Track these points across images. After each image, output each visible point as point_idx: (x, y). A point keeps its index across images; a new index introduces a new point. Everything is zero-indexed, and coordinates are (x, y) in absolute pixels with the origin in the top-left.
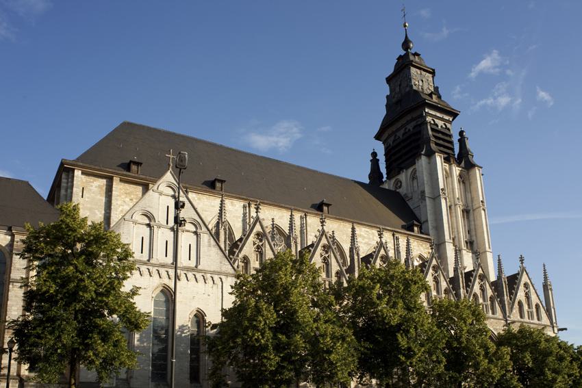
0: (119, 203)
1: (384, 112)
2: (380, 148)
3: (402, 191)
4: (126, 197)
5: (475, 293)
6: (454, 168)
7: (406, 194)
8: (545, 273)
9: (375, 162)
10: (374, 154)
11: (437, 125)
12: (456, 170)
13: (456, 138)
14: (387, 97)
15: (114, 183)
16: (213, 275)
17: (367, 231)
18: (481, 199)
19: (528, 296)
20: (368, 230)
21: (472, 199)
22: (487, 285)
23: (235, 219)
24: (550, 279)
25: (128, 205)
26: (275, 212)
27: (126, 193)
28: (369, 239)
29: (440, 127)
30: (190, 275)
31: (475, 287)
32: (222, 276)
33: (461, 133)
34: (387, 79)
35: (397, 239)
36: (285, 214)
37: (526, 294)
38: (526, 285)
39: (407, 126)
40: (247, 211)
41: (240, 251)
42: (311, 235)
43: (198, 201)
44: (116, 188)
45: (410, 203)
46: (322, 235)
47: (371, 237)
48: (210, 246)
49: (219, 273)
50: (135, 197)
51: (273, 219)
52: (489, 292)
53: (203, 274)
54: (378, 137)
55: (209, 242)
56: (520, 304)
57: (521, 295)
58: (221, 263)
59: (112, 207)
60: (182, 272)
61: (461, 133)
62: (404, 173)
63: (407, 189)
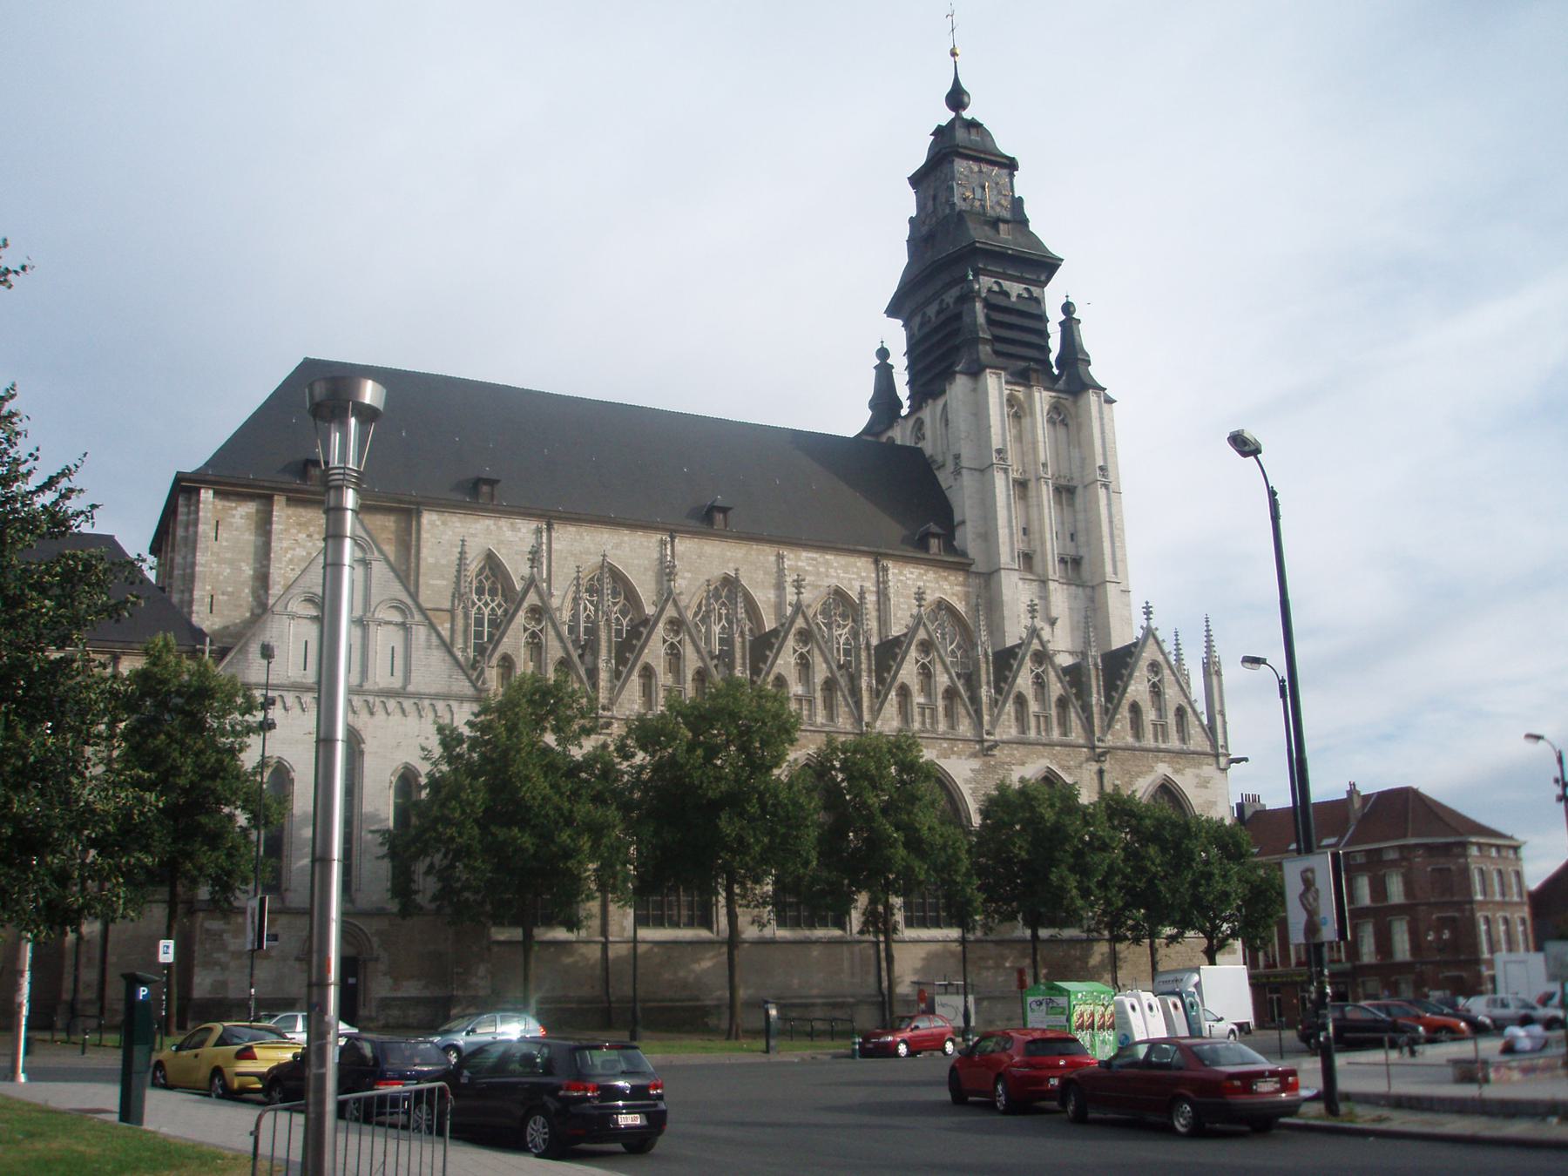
0: (285, 544)
1: (902, 259)
2: (896, 336)
3: (928, 447)
4: (299, 532)
6: (1037, 395)
7: (931, 456)
8: (1208, 636)
9: (884, 372)
10: (883, 353)
11: (1006, 294)
12: (1042, 399)
13: (1054, 317)
14: (912, 220)
15: (276, 508)
16: (434, 702)
17: (813, 559)
18: (1100, 462)
19: (1156, 691)
20: (815, 555)
21: (1083, 460)
22: (1052, 674)
23: (519, 557)
25: (304, 547)
26: (606, 536)
27: (299, 524)
28: (818, 574)
29: (1014, 299)
30: (392, 704)
31: (1019, 681)
32: (452, 703)
33: (1068, 308)
35: (885, 569)
36: (626, 538)
37: (1154, 685)
38: (1154, 667)
39: (944, 297)
40: (544, 539)
41: (494, 650)
42: (684, 578)
43: (441, 528)
44: (279, 516)
46: (667, 600)
47: (822, 570)
48: (429, 647)
49: (446, 697)
51: (578, 567)
52: (1056, 689)
53: (416, 701)
54: (893, 310)
55: (428, 640)
56: (1135, 708)
57: (1138, 689)
58: (450, 677)
59: (272, 555)
60: (378, 700)
61: (1068, 308)
62: (928, 408)
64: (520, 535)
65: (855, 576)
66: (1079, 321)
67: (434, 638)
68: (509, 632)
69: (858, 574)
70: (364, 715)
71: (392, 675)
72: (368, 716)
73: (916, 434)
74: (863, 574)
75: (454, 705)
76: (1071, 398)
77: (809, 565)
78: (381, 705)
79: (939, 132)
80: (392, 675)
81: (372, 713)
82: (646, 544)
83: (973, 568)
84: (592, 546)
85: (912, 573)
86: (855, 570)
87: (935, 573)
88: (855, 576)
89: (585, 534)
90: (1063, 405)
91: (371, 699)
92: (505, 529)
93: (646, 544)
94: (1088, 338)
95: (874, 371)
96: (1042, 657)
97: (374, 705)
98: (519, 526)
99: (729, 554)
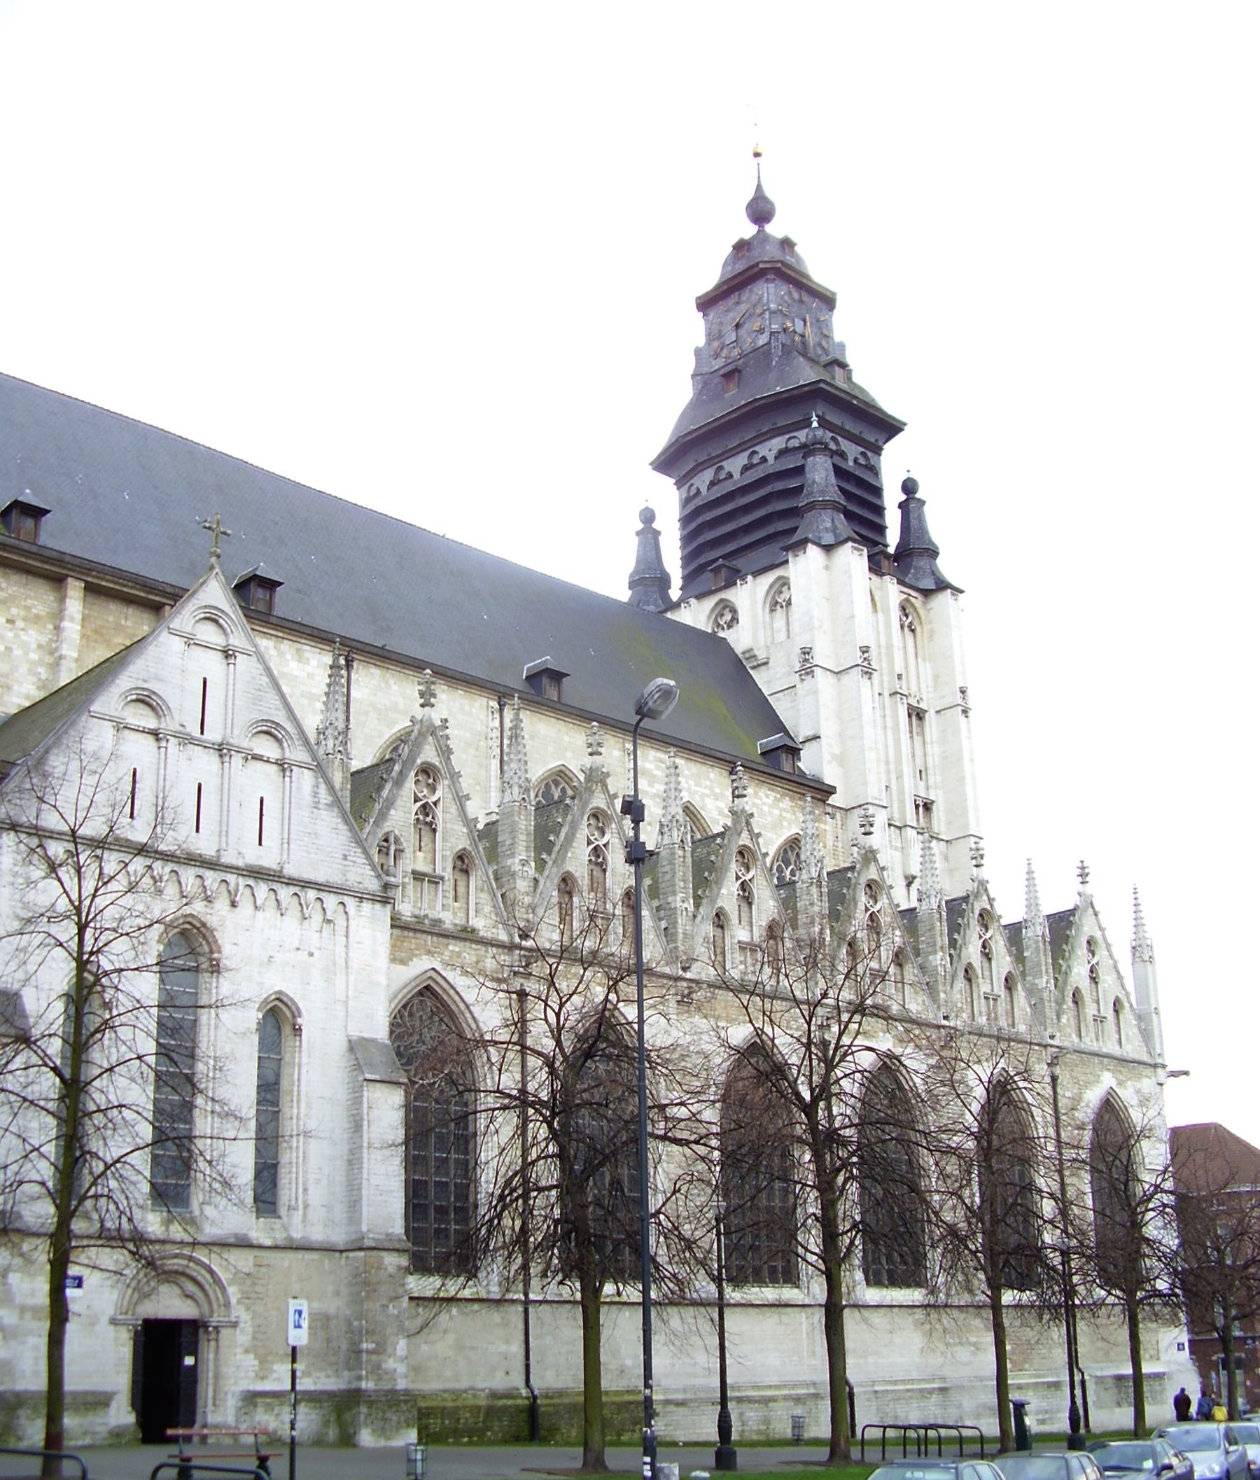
3: (740, 639)
5: (970, 964)
10: (648, 517)
13: (892, 497)
24: (1152, 932)
30: (262, 889)
32: (346, 899)
33: (909, 487)
34: (698, 298)
45: (759, 677)
48: (316, 805)
50: (23, 613)
52: (1003, 962)
53: (297, 889)
54: (667, 463)
58: (345, 857)
60: (242, 882)
61: (909, 487)
63: (755, 635)
64: (309, 669)
65: (707, 792)
66: (923, 503)
67: (323, 789)
68: (399, 803)
69: (712, 790)
70: (222, 904)
71: (260, 844)
72: (228, 908)
73: (716, 620)
74: (717, 790)
75: (351, 903)
76: (920, 597)
77: (657, 768)
78: (248, 891)
79: (741, 247)
80: (260, 844)
81: (233, 904)
82: (467, 708)
83: (832, 800)
84: (401, 700)
85: (767, 796)
86: (708, 783)
87: (792, 799)
88: (707, 792)
89: (392, 681)
90: (913, 605)
91: (232, 878)
92: (288, 657)
93: (467, 708)
94: (937, 526)
95: (636, 539)
96: (986, 918)
97: (237, 891)
98: (307, 655)
99: (566, 738)
